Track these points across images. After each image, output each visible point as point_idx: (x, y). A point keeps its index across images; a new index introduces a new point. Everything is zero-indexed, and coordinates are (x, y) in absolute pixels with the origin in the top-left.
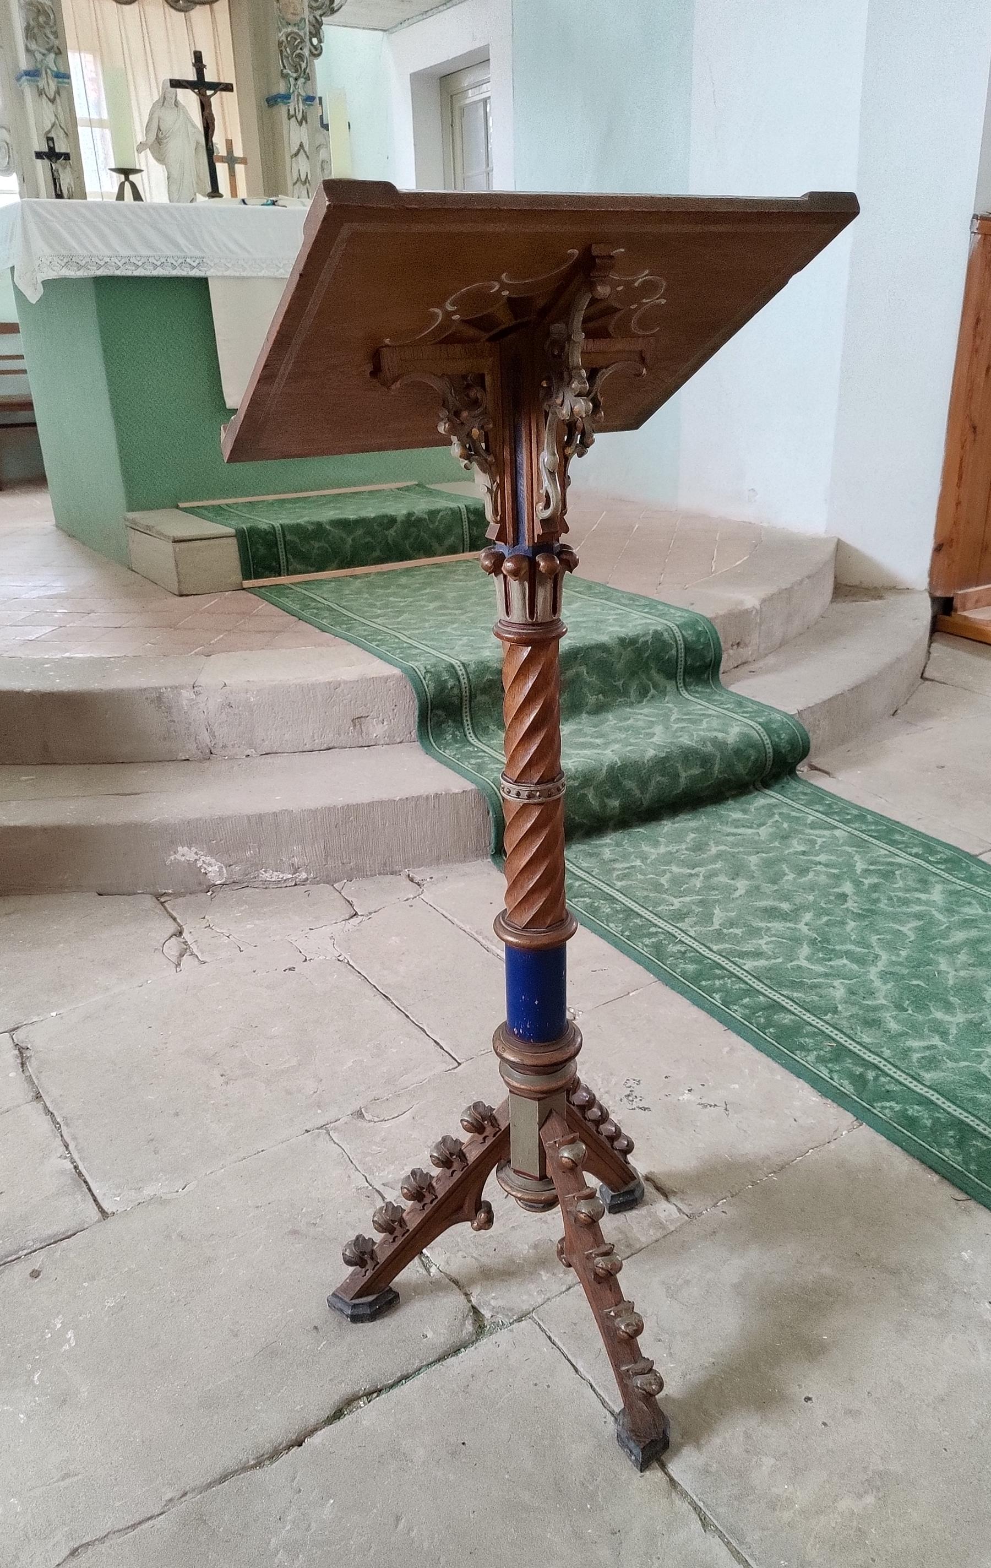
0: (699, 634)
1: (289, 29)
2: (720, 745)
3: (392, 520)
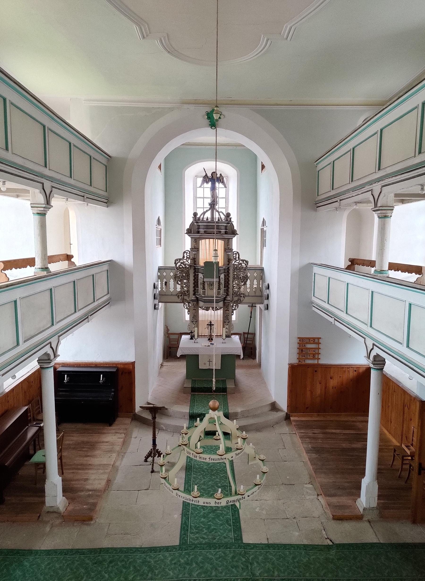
0: (226, 414)
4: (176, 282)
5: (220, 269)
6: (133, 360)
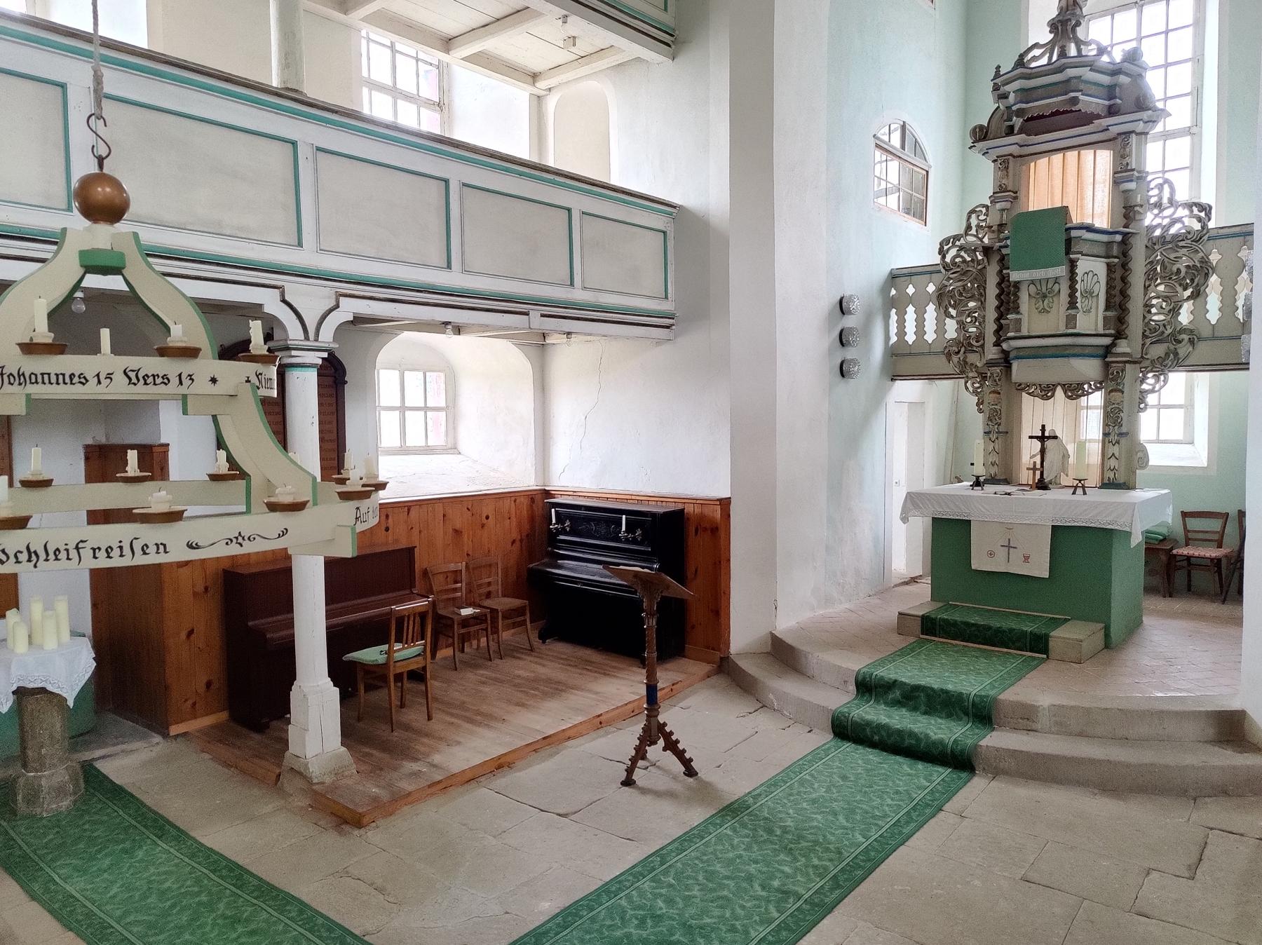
1: (1113, 406)
2: (927, 736)
3: (990, 628)
4: (942, 311)
5: (1074, 233)
6: (725, 494)
